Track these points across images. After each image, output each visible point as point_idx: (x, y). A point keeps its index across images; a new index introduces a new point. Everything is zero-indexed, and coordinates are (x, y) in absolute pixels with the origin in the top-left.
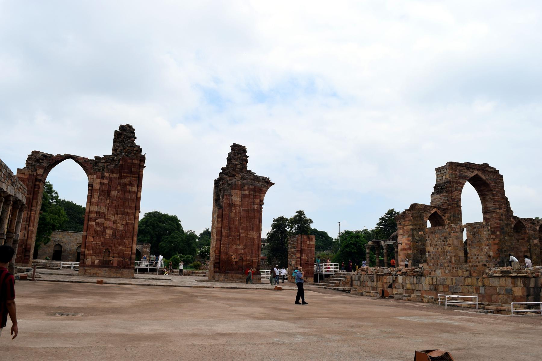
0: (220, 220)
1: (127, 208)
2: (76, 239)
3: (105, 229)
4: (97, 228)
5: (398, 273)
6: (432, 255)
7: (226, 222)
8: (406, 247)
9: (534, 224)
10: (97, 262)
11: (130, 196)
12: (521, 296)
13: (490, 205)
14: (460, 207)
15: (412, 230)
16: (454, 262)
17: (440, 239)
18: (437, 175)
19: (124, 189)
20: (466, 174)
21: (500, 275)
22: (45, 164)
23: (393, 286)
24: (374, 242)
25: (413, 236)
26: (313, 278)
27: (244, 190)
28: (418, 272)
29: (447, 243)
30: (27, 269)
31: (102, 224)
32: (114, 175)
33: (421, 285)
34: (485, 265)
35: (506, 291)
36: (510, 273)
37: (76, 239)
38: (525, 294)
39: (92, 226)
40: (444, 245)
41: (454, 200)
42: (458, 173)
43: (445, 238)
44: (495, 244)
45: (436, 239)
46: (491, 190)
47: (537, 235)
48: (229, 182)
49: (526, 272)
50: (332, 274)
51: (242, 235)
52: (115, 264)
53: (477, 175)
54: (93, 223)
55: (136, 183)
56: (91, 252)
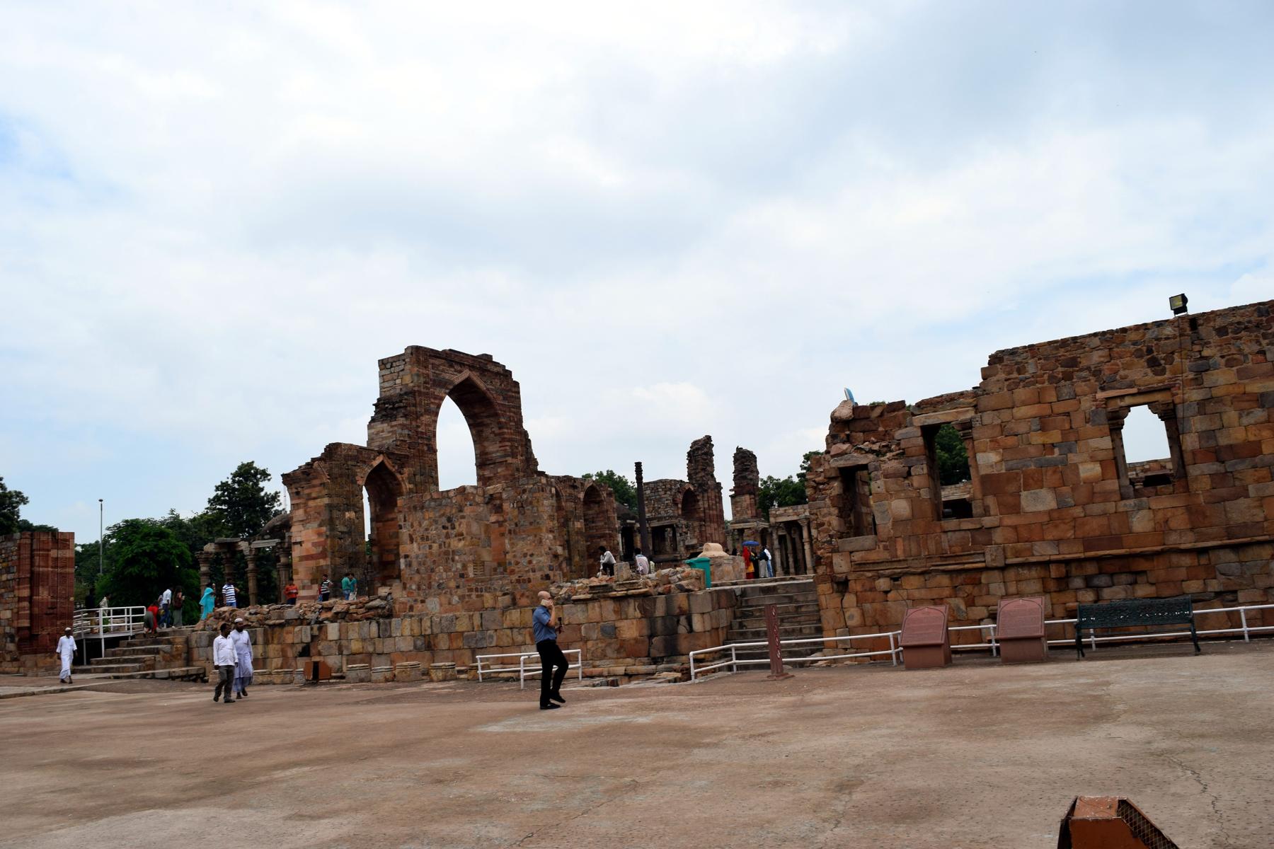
5: (324, 616)
8: (314, 551)
9: (574, 487)
12: (635, 639)
13: (493, 448)
14: (435, 451)
15: (330, 507)
16: (471, 575)
17: (436, 522)
18: (381, 376)
20: (447, 376)
21: (589, 596)
23: (313, 651)
24: (221, 545)
25: (331, 522)
28: (377, 608)
29: (454, 532)
33: (389, 641)
34: (547, 577)
35: (603, 630)
36: (612, 589)
38: (646, 632)
40: (447, 536)
41: (420, 435)
42: (430, 372)
43: (449, 520)
45: (425, 523)
46: (496, 415)
47: (580, 512)
49: (646, 585)
50: (126, 638)
53: (468, 379)
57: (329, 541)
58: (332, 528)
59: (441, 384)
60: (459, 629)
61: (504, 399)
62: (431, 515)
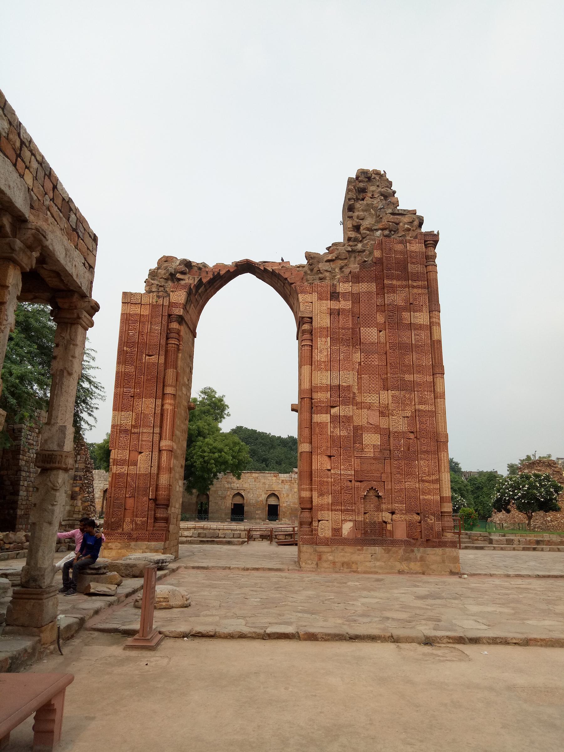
1: (411, 369)
2: (264, 483)
3: (358, 432)
4: (337, 432)
10: (347, 528)
11: (414, 337)
19: (394, 319)
22: (189, 280)
30: (157, 562)
31: (349, 419)
32: (363, 287)
37: (264, 483)
39: (321, 425)
52: (401, 533)
54: (324, 418)
55: (424, 300)
56: (328, 499)
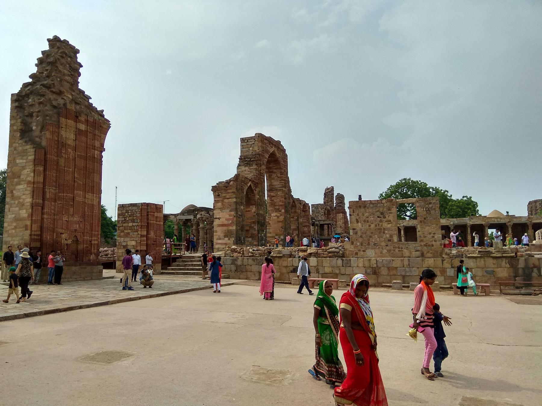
0: (41, 169)
6: (359, 233)
7: (52, 174)
8: (226, 222)
9: (300, 204)
15: (236, 203)
17: (374, 214)
21: (479, 255)
25: (236, 210)
26: (160, 265)
27: (80, 121)
40: (381, 221)
43: (382, 214)
44: (279, 222)
45: (366, 214)
46: (281, 168)
48: (55, 103)
51: (77, 199)
57: (235, 219)
58: (237, 213)
59: (267, 152)
60: (394, 265)
61: (283, 162)
62: (371, 210)
